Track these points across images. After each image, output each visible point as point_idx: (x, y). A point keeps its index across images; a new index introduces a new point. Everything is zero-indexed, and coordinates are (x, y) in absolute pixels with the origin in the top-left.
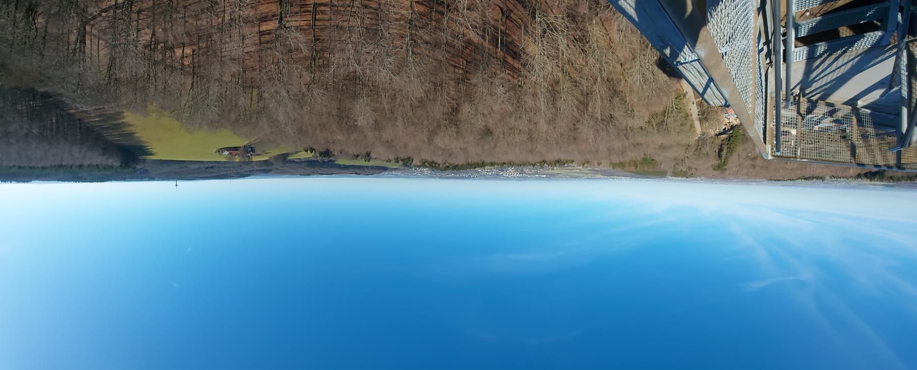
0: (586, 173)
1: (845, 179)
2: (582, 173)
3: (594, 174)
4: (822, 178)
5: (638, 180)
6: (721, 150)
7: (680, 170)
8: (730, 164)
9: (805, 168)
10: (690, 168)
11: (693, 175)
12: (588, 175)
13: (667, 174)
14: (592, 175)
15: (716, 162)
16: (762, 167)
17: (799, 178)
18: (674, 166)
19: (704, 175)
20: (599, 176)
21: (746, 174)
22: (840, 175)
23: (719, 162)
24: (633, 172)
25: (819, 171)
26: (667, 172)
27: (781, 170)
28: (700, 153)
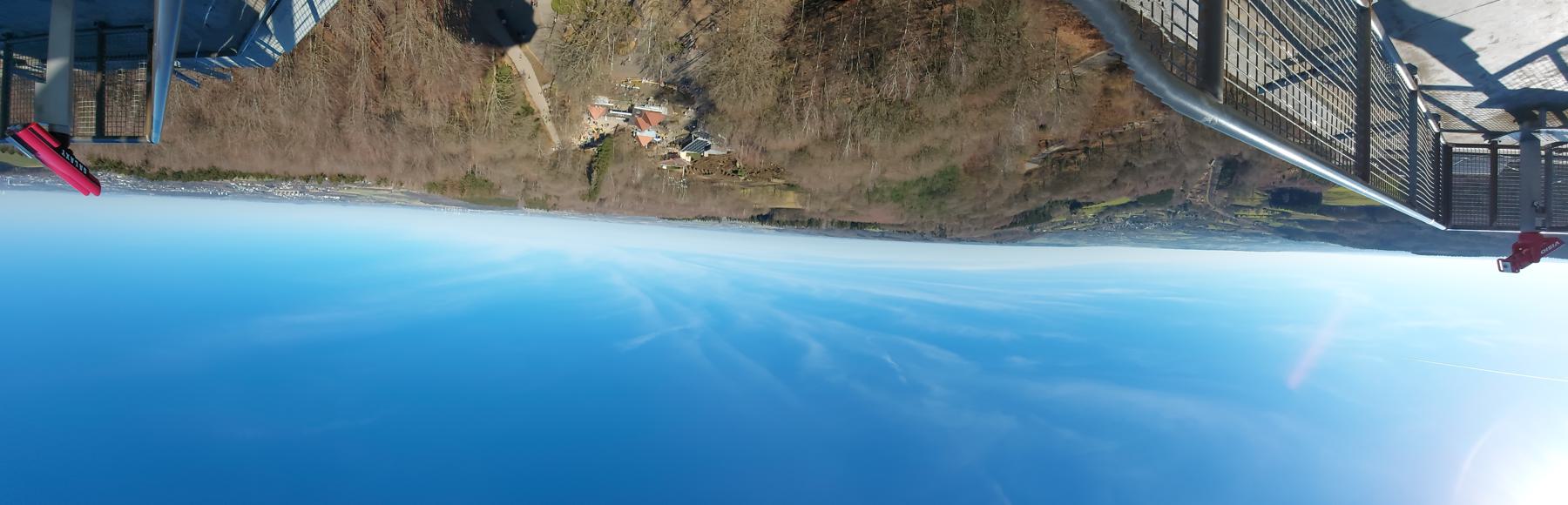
1: (740, 222)
4: (719, 219)
8: (603, 193)
9: (699, 205)
15: (585, 188)
17: (696, 218)
22: (734, 216)
25: (713, 209)
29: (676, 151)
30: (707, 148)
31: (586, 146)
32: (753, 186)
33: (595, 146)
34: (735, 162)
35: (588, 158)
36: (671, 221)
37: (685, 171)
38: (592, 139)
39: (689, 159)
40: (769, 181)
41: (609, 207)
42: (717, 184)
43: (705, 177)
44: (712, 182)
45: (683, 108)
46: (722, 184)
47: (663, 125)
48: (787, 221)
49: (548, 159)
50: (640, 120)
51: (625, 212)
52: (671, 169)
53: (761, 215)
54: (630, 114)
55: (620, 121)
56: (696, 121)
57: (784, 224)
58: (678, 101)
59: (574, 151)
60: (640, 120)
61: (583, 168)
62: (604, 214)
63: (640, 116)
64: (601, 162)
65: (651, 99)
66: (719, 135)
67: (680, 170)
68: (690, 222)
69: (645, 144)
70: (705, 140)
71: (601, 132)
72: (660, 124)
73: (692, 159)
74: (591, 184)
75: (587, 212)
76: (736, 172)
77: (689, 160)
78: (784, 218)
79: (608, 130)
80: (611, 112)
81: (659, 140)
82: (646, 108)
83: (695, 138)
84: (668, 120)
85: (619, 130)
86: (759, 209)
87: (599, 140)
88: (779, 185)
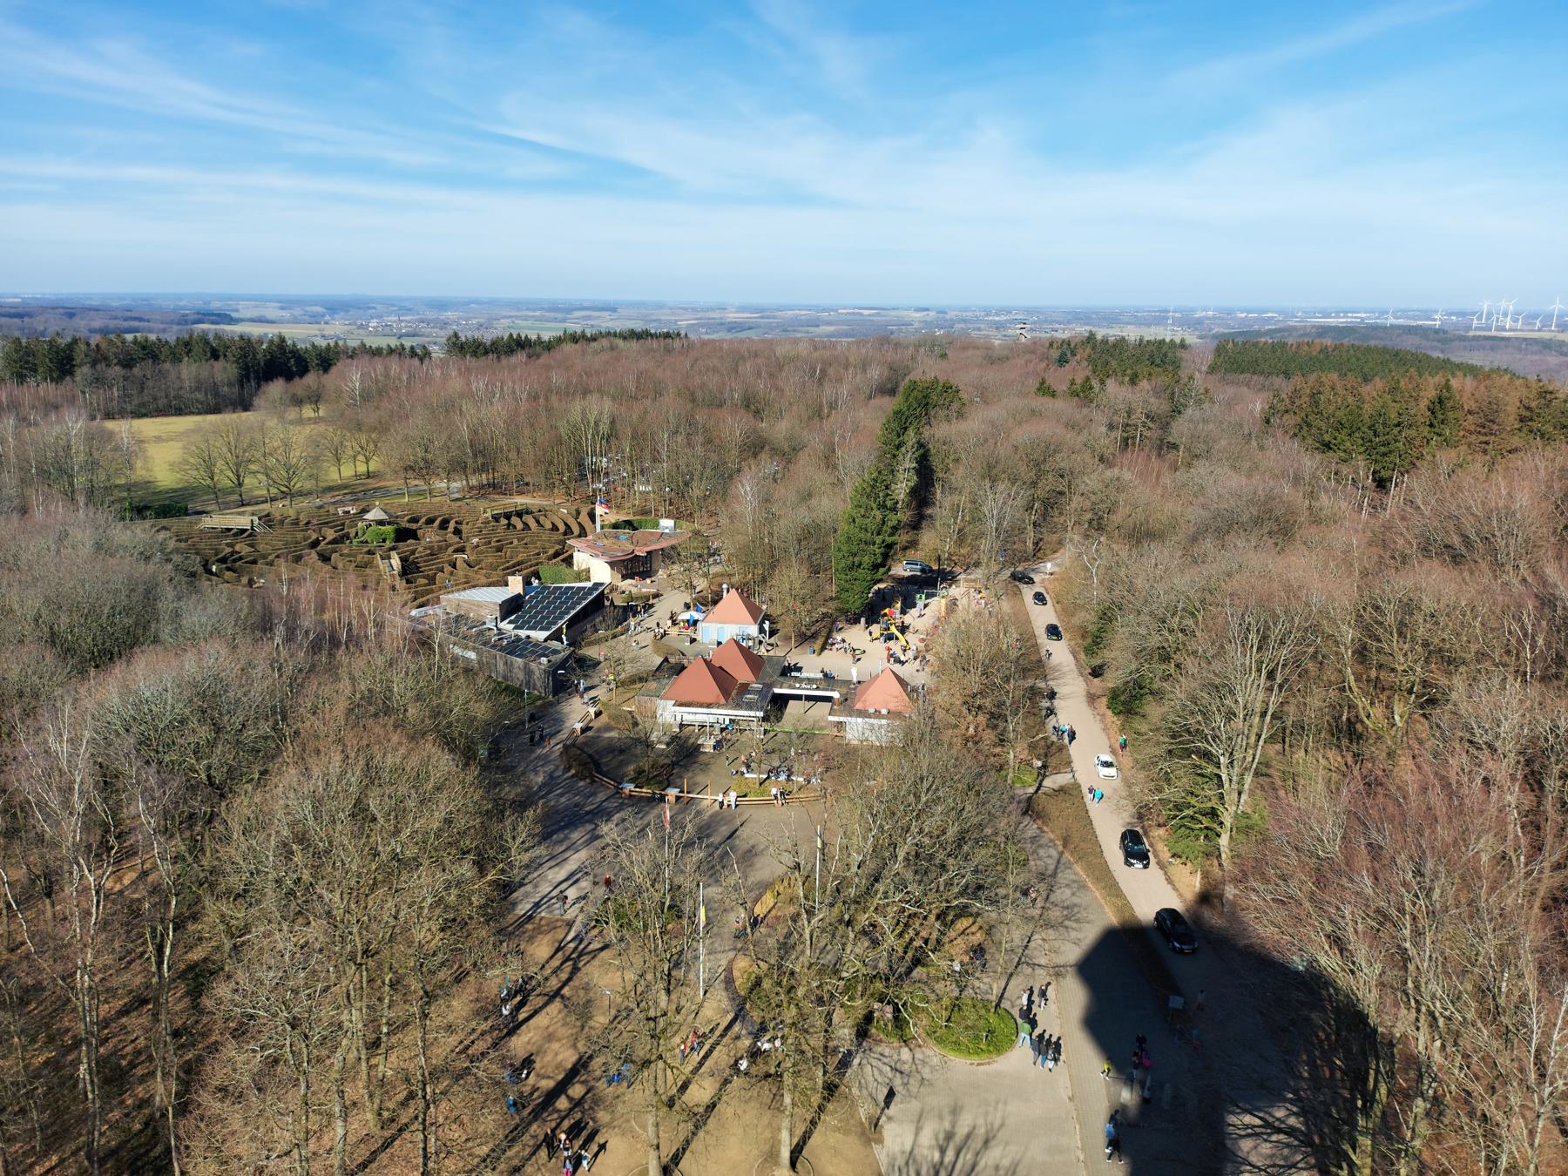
1: (374, 342)
5: (1403, 313)
6: (922, 496)
8: (874, 417)
10: (1083, 393)
11: (1055, 354)
13: (1210, 358)
18: (1177, 411)
21: (780, 367)
23: (926, 433)
24: (1472, 370)
26: (1213, 369)
28: (1034, 484)
29: (628, 586)
30: (511, 607)
31: (930, 580)
32: (330, 489)
33: (901, 581)
34: (409, 569)
36: (638, 326)
37: (592, 516)
38: (908, 604)
39: (581, 559)
40: (267, 519)
41: (864, 365)
42: (474, 481)
43: (521, 501)
44: (494, 487)
45: (608, 728)
47: (673, 668)
48: (176, 359)
50: (742, 674)
51: (803, 349)
53: (289, 377)
54: (777, 691)
55: (811, 663)
56: (555, 693)
57: (187, 346)
58: (622, 750)
59: (977, 564)
60: (742, 674)
61: (943, 504)
63: (745, 688)
65: (708, 744)
66: (472, 655)
67: (613, 518)
68: (576, 328)
69: (731, 599)
71: (876, 629)
72: (683, 668)
73: (569, 561)
74: (921, 445)
75: (940, 348)
76: (403, 535)
78: (188, 371)
79: (857, 635)
80: (836, 695)
81: (686, 616)
82: (723, 714)
83: (556, 636)
84: (653, 685)
85: (818, 635)
86: (298, 402)
87: (884, 599)
88: (224, 507)
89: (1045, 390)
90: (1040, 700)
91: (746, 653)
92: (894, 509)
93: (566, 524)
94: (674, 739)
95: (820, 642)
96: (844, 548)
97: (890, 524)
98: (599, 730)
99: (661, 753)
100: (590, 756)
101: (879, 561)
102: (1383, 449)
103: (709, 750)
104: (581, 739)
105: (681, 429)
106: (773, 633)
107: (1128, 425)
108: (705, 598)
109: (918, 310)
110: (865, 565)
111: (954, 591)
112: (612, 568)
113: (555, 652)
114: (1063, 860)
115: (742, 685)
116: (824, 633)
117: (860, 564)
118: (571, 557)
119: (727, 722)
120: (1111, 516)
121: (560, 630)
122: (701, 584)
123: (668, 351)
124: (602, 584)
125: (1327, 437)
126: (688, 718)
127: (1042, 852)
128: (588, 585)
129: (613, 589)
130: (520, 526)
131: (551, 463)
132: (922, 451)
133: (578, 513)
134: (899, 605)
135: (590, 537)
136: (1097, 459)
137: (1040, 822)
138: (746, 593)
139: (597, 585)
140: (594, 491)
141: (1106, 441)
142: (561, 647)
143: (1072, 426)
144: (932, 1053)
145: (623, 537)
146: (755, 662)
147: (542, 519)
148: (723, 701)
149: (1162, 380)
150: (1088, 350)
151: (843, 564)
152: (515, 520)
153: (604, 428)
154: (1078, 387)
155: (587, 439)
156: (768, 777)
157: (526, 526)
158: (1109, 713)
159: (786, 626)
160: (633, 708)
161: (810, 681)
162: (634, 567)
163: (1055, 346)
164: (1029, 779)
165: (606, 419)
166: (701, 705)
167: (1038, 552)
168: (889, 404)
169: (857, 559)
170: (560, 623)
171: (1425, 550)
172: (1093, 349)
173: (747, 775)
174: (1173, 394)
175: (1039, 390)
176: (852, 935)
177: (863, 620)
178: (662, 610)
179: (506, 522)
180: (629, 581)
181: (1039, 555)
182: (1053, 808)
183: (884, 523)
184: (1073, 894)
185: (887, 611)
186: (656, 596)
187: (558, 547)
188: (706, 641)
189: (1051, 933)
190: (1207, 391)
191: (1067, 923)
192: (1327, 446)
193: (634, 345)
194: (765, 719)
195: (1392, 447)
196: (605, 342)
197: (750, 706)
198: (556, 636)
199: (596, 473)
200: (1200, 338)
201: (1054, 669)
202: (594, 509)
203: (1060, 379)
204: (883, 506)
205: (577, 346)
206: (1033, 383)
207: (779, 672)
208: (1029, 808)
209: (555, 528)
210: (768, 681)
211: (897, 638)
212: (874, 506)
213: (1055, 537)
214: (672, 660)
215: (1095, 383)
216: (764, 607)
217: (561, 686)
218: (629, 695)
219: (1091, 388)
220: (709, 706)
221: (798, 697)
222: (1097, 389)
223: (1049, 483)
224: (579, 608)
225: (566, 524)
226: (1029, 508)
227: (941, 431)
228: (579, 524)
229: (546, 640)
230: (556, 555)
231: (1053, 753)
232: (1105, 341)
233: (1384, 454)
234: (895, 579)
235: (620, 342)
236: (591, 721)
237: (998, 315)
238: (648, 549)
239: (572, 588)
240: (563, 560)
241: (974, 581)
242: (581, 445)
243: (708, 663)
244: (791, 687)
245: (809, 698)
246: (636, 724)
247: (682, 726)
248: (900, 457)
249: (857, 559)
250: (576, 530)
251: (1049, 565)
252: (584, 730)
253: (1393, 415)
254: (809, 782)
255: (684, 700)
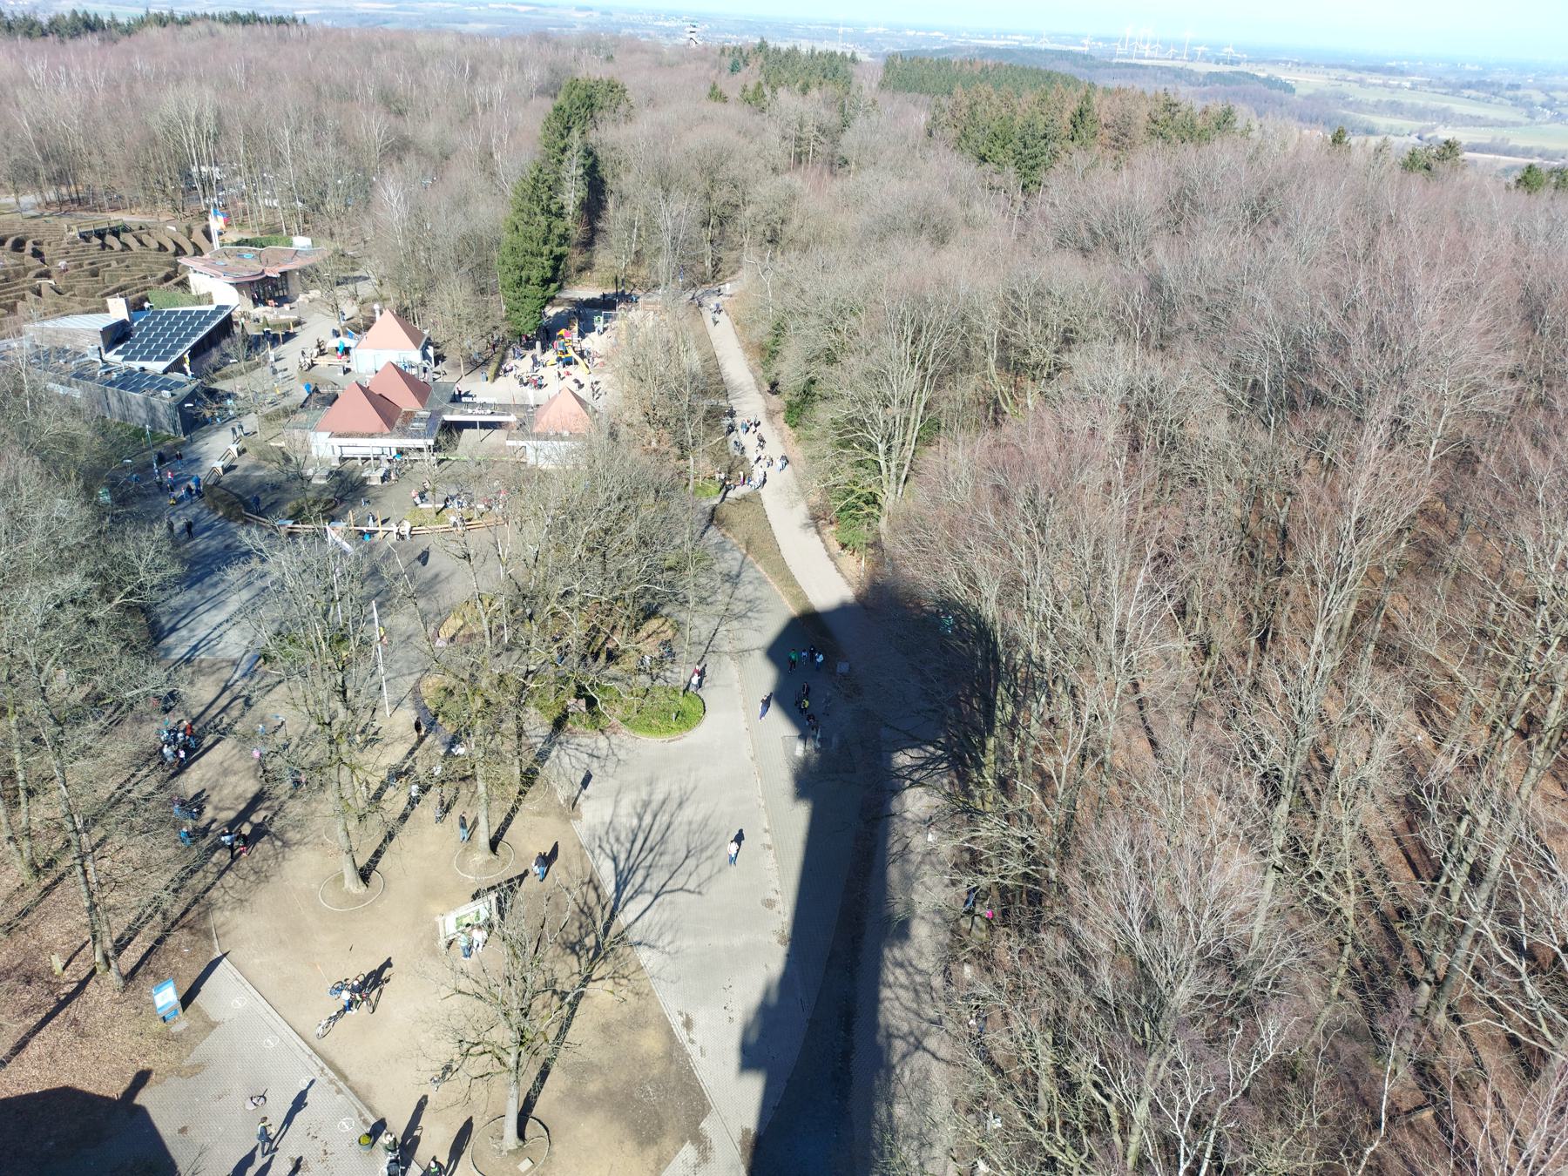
0: (1395, 108)
2: (1420, 114)
3: (1342, 98)
6: (594, 205)
7: (814, 93)
10: (755, 100)
11: (727, 62)
12: (1386, 96)
14: (1356, 93)
16: (345, 95)
17: (128, 31)
19: (660, 62)
20: (1307, 82)
21: (423, 63)
26: (882, 86)
27: (239, 77)
30: (117, 336)
31: (606, 304)
35: (603, 257)
37: (207, 234)
39: (200, 282)
41: (521, 64)
45: (257, 467)
46: (29, 199)
49: (750, 256)
50: (406, 400)
52: (276, 231)
54: (448, 418)
55: (486, 391)
59: (656, 285)
60: (406, 400)
61: (614, 216)
62: (542, 38)
63: (409, 416)
64: (538, 234)
65: (375, 478)
67: (233, 236)
69: (387, 323)
70: (136, 365)
71: (551, 356)
72: (337, 397)
73: (184, 284)
75: (604, 45)
77: (194, 280)
80: (512, 418)
81: (333, 343)
83: (177, 366)
84: (302, 417)
85: (490, 361)
87: (563, 321)
89: (716, 95)
90: (719, 417)
91: (410, 381)
92: (560, 214)
93: (175, 243)
94: (334, 474)
95: (493, 367)
96: (510, 260)
97: (557, 232)
98: (246, 469)
99: (324, 489)
100: (237, 495)
101: (549, 275)
102: (1031, 162)
103: (376, 482)
104: (226, 478)
105: (305, 126)
106: (439, 358)
107: (801, 139)
108: (357, 325)
109: (579, 9)
110: (533, 280)
111: (635, 315)
112: (240, 292)
113: (179, 384)
114: (746, 561)
115: (407, 413)
116: (497, 358)
117: (528, 279)
118: (186, 279)
119: (394, 453)
120: (785, 229)
121: (181, 360)
122: (350, 309)
123: (282, 39)
124: (226, 307)
125: (983, 150)
126: (348, 452)
127: (727, 556)
128: (212, 308)
129: (245, 315)
130: (117, 245)
131: (146, 169)
132: (590, 161)
133: (190, 230)
134: (576, 328)
135: (207, 256)
136: (770, 171)
137: (723, 530)
138: (403, 314)
139: (220, 308)
140: (208, 206)
141: (780, 152)
142: (187, 380)
143: (745, 133)
144: (625, 736)
145: (248, 256)
146: (421, 390)
147: (145, 238)
148: (387, 431)
149: (830, 89)
150: (761, 59)
151: (510, 279)
152: (110, 239)
153: (209, 125)
154: (750, 95)
155: (189, 140)
156: (445, 507)
157: (126, 246)
158: (786, 426)
159: (452, 354)
160: (282, 444)
161: (483, 405)
162: (267, 290)
163: (727, 52)
164: (714, 488)
165: (209, 113)
166: (363, 436)
167: (717, 272)
168: (548, 105)
169: (524, 274)
170: (180, 352)
171: (1060, 244)
172: (766, 58)
173: (421, 506)
174: (843, 106)
175: (710, 96)
176: (535, 628)
177: (538, 344)
178: (305, 340)
179: (100, 241)
180: (261, 309)
181: (719, 276)
182: (734, 515)
183: (550, 231)
184: (756, 589)
185: (562, 332)
186: (298, 323)
187: (169, 269)
188: (362, 370)
189: (735, 624)
190: (874, 103)
191: (749, 614)
192: (983, 159)
193: (239, 30)
194: (437, 448)
195: (1039, 160)
196: (201, 27)
197: (416, 434)
198: (177, 366)
199: (207, 182)
200: (871, 56)
201: (736, 389)
202: (208, 226)
203: (731, 86)
204: (547, 211)
205: (166, 31)
206: (705, 89)
207: (448, 399)
208: (713, 517)
209: (162, 248)
210: (437, 408)
211: (576, 363)
212: (538, 210)
213: (734, 255)
214: (323, 390)
215: (767, 91)
216: (426, 332)
217: (193, 422)
218: (276, 431)
219: (764, 96)
220: (371, 436)
221: (471, 425)
222: (768, 98)
223: (722, 194)
224: (201, 334)
225: (175, 243)
226: (706, 224)
227: (608, 135)
228: (194, 244)
229: (165, 372)
230: (167, 278)
231: (734, 469)
232: (777, 51)
233: (1032, 168)
234: (570, 301)
235: (221, 27)
236: (234, 459)
237: (666, 19)
238: (282, 269)
239: (191, 312)
240: (177, 284)
241: (655, 304)
242: (182, 146)
243: (366, 391)
244: (462, 413)
245: (485, 425)
246: (288, 460)
247: (343, 460)
248: (566, 163)
249: (524, 274)
250: (189, 249)
251: (728, 285)
252: (226, 470)
253: (1041, 126)
254: (490, 508)
255: (342, 431)
